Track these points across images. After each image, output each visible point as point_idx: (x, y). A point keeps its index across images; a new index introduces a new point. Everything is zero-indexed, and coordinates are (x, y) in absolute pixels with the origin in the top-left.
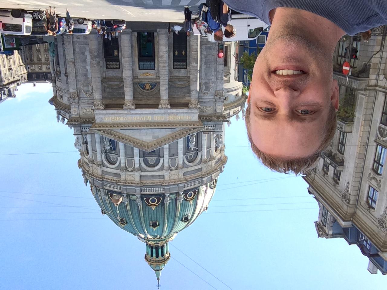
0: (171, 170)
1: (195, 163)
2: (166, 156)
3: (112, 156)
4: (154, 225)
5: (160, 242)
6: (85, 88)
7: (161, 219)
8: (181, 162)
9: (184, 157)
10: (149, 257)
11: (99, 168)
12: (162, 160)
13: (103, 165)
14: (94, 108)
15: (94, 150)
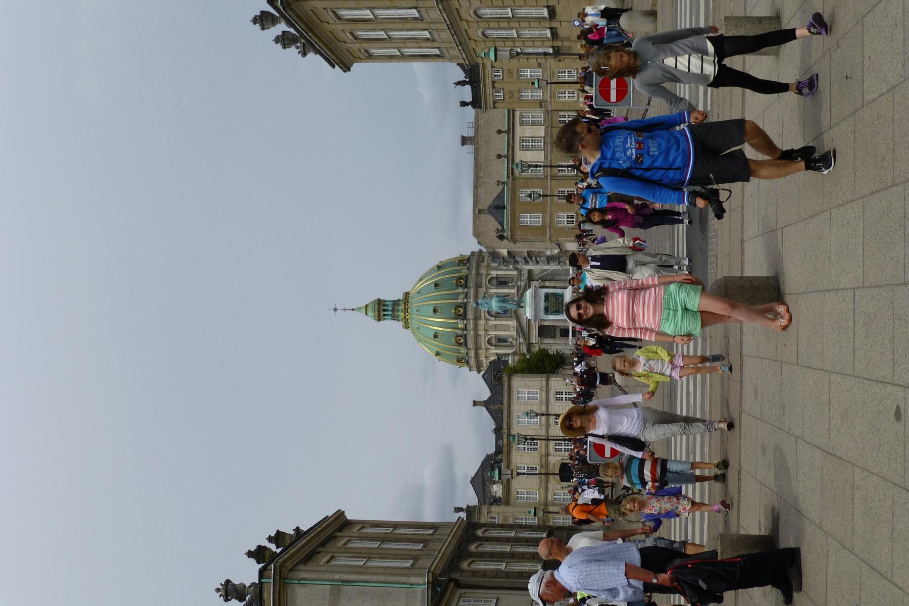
0: (485, 326)
1: (487, 343)
2: (496, 322)
3: (494, 282)
4: (435, 311)
5: (403, 314)
6: (549, 274)
7: (441, 316)
8: (490, 333)
9: (494, 335)
10: (382, 303)
11: (485, 271)
12: (494, 319)
13: (487, 275)
14: (540, 281)
15: (497, 269)
